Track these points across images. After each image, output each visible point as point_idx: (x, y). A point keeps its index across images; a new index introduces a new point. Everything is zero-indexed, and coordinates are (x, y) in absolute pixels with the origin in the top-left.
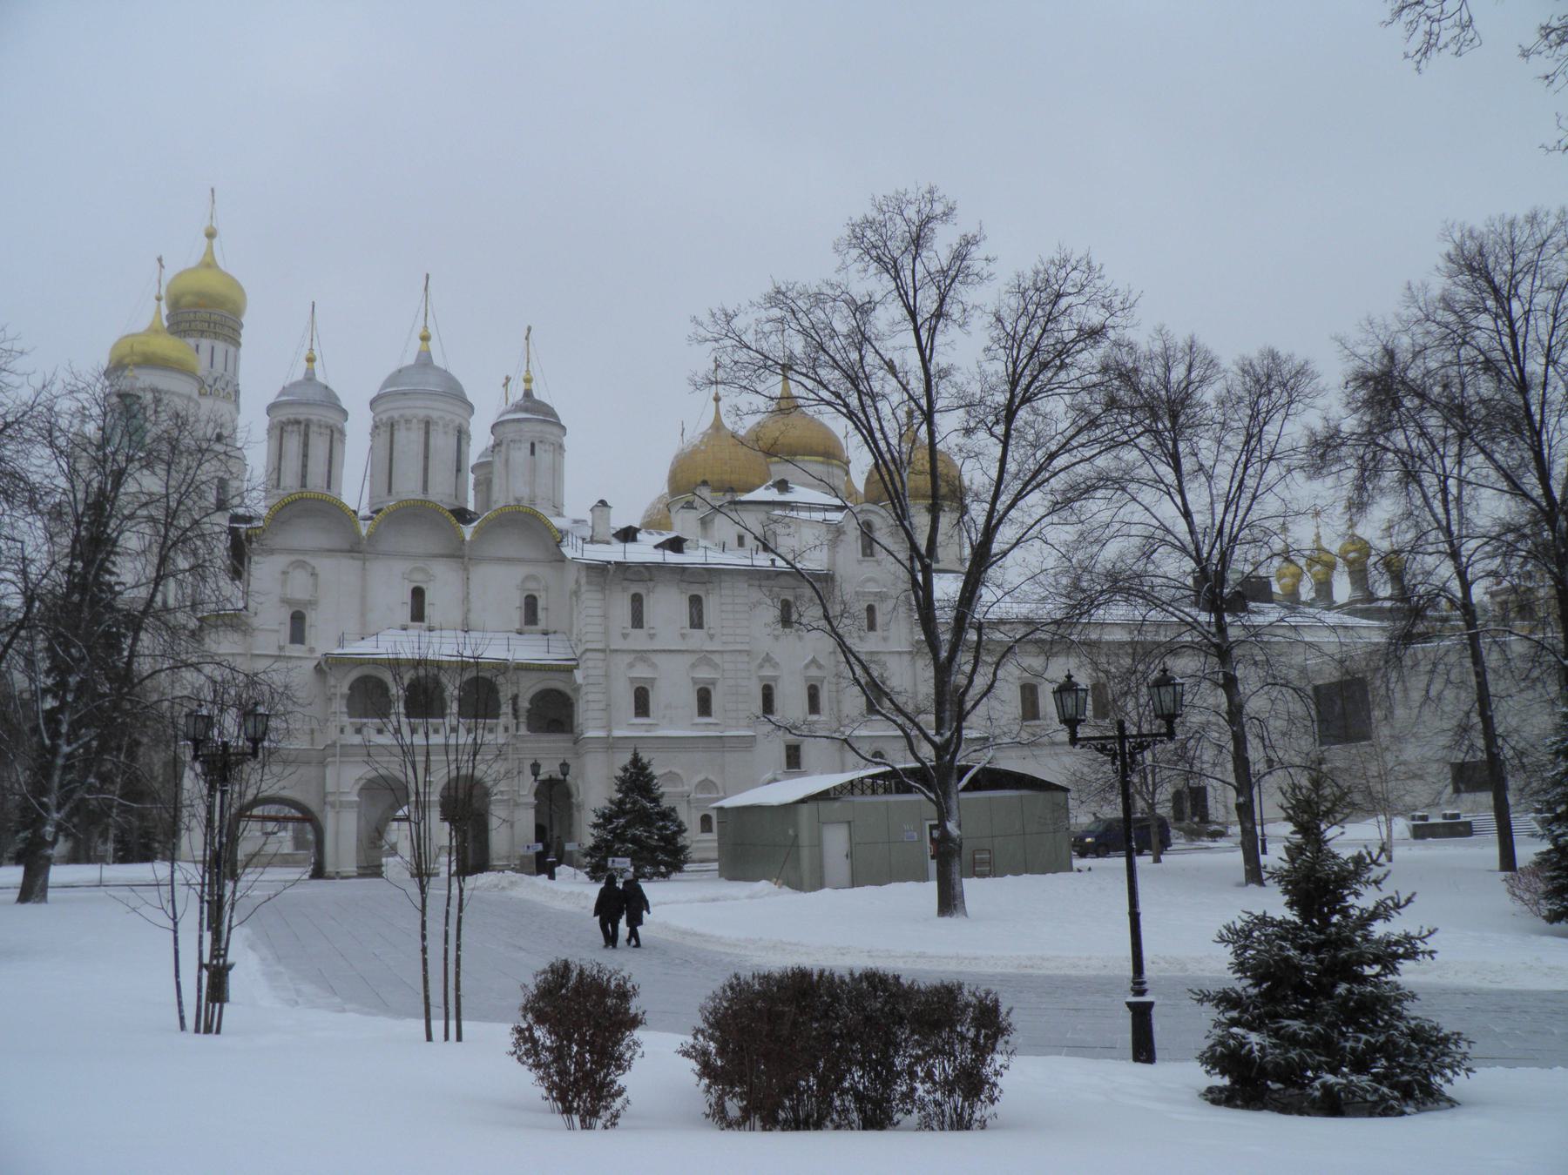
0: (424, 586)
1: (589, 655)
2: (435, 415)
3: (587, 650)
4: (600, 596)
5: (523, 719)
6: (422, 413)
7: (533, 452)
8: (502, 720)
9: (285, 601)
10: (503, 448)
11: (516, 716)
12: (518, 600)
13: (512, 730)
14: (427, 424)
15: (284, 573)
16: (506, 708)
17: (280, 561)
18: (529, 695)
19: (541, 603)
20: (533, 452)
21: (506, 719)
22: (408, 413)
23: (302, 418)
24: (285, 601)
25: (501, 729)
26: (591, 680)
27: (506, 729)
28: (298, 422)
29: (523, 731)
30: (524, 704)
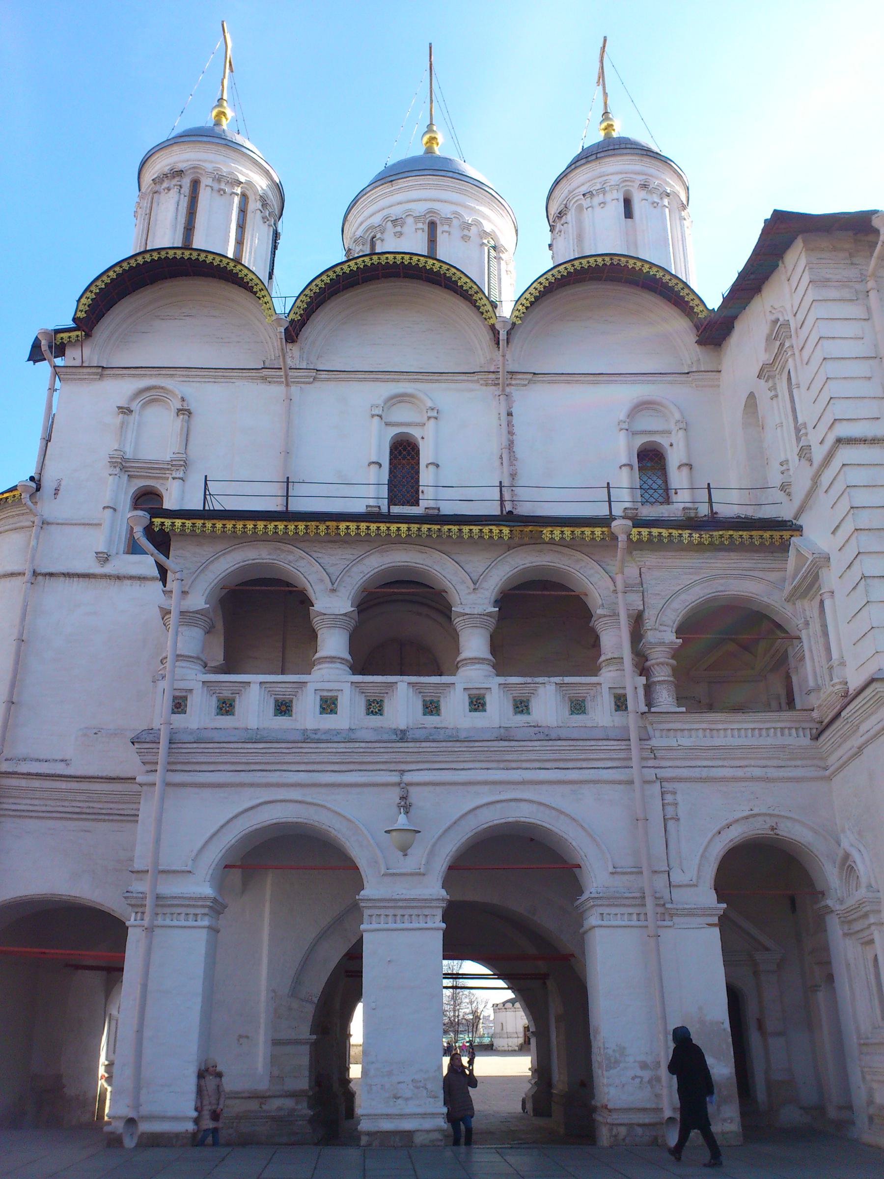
0: (416, 432)
1: (846, 454)
2: (445, 210)
3: (839, 441)
4: (854, 310)
5: (662, 674)
6: (420, 208)
7: (629, 213)
8: (607, 677)
9: (123, 465)
10: (570, 217)
11: (643, 668)
12: (622, 449)
13: (636, 702)
14: (432, 226)
15: (125, 411)
16: (614, 640)
17: (120, 390)
18: (674, 614)
19: (674, 458)
20: (629, 213)
21: (616, 673)
22: (396, 211)
23: (181, 166)
24: (123, 465)
25: (606, 701)
26: (865, 519)
27: (620, 703)
28: (180, 173)
29: (665, 698)
30: (663, 635)
